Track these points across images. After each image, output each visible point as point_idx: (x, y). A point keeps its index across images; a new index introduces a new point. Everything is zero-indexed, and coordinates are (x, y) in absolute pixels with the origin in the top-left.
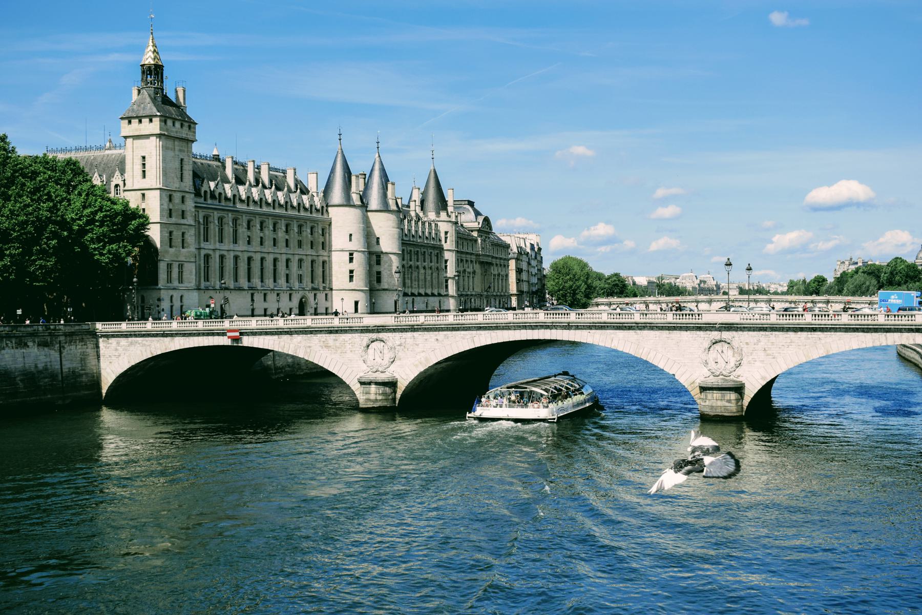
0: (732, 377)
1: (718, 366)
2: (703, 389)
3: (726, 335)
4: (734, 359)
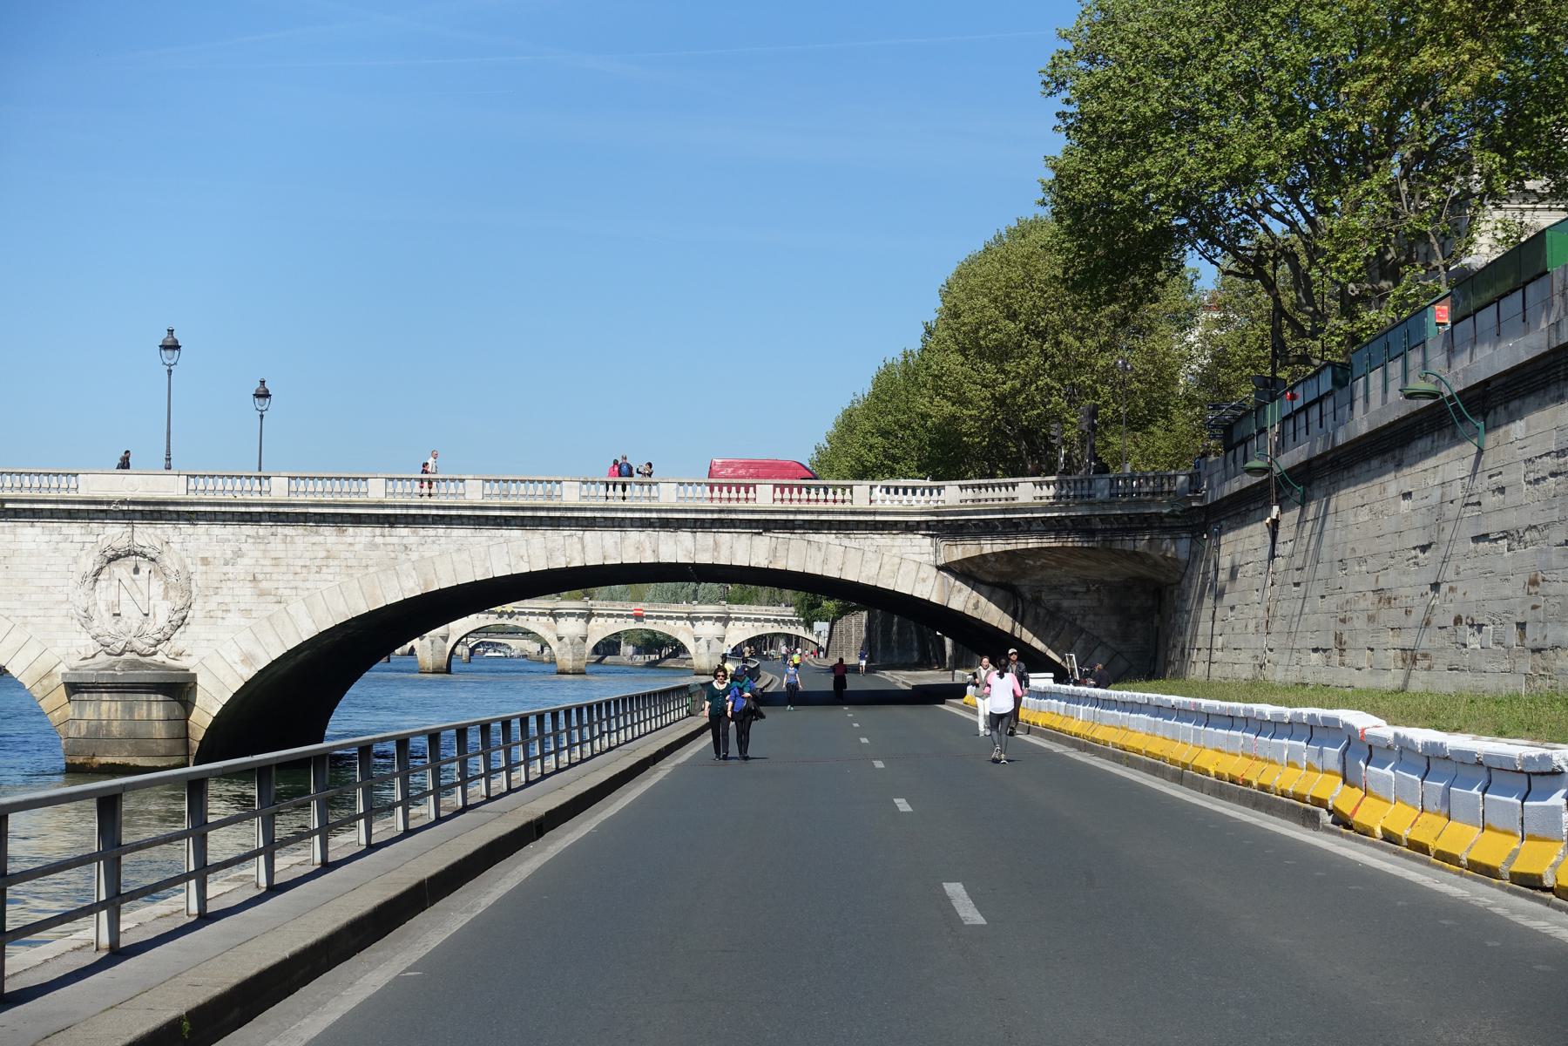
0: (159, 658)
2: (74, 688)
3: (147, 535)
4: (168, 605)
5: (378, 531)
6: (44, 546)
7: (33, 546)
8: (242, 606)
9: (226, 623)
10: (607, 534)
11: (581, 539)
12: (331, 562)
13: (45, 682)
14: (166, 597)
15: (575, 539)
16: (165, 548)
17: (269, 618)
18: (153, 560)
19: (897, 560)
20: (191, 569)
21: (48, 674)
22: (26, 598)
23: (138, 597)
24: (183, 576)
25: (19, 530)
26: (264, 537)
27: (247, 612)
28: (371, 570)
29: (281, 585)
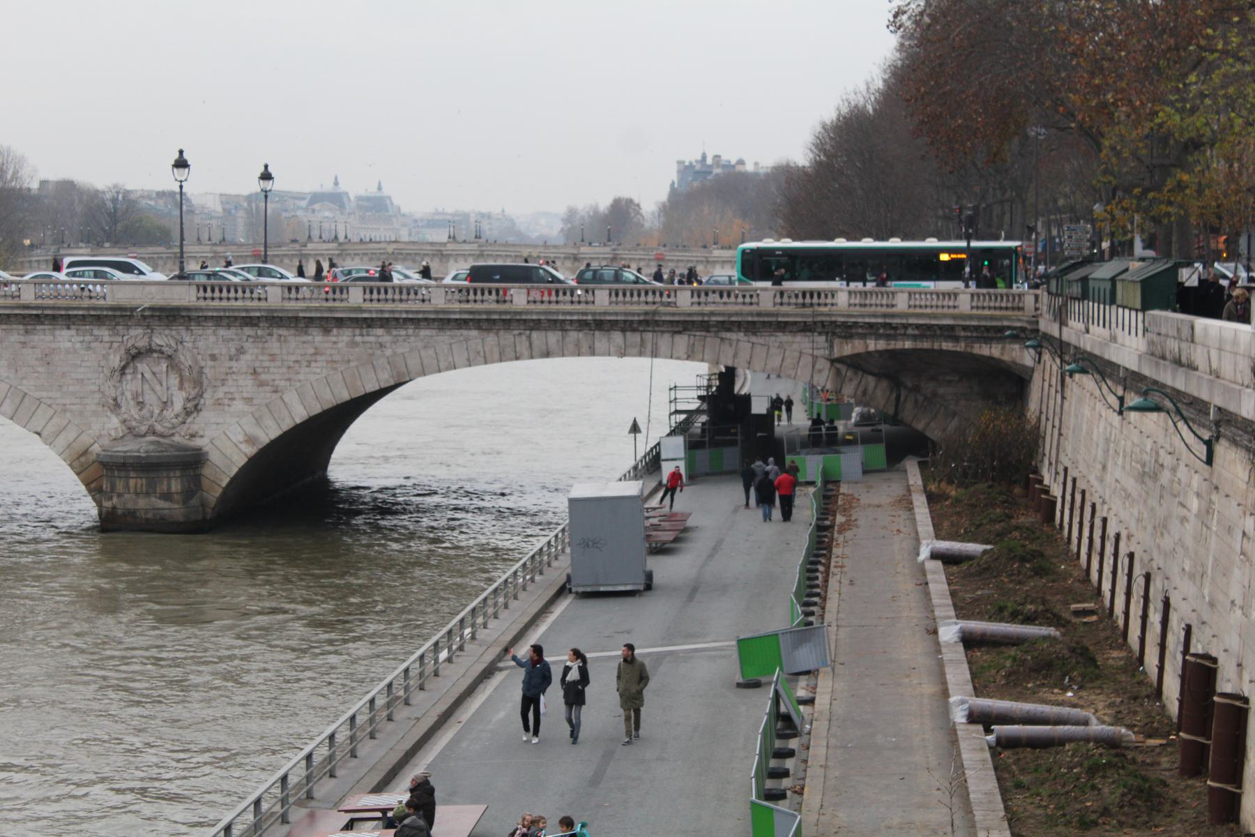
0: (177, 438)
1: (145, 412)
3: (162, 338)
5: (357, 331)
6: (78, 345)
7: (69, 345)
8: (245, 395)
9: (232, 409)
10: (550, 334)
11: (529, 337)
12: (319, 358)
13: (83, 459)
14: (181, 388)
15: (524, 338)
16: (180, 347)
17: (267, 405)
18: (170, 357)
19: (797, 354)
20: (203, 363)
21: (85, 452)
22: (65, 389)
23: (158, 388)
24: (195, 371)
25: (57, 332)
26: (262, 337)
27: (249, 400)
28: (353, 364)
29: (278, 377)
